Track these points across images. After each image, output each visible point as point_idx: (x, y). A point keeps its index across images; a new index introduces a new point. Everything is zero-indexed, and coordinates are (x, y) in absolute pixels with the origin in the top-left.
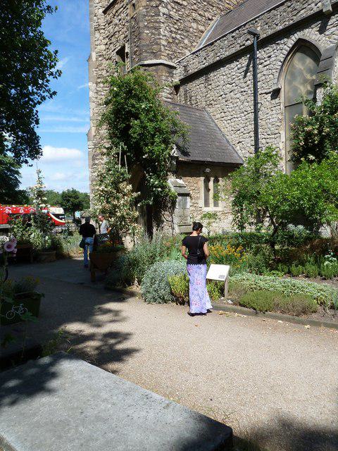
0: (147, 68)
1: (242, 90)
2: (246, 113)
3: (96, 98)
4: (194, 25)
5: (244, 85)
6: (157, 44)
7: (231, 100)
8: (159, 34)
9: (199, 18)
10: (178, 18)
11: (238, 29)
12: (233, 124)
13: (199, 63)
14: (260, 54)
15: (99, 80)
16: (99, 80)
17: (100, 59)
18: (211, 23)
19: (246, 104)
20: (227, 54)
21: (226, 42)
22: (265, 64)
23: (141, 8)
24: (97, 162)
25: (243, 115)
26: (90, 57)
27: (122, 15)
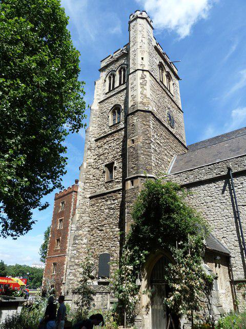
0: (143, 179)
1: (222, 201)
2: (226, 217)
3: (83, 193)
4: (166, 157)
5: (223, 198)
6: (149, 165)
7: (212, 207)
8: (151, 159)
9: (167, 154)
10: (159, 152)
11: (213, 164)
12: (216, 224)
13: (181, 180)
14: (235, 181)
15: (86, 181)
16: (86, 181)
17: (89, 167)
18: (173, 158)
19: (225, 211)
20: (206, 178)
21: (203, 171)
22: (239, 187)
23: (139, 143)
24: (77, 242)
25: (224, 218)
26: (82, 165)
27: (112, 144)
